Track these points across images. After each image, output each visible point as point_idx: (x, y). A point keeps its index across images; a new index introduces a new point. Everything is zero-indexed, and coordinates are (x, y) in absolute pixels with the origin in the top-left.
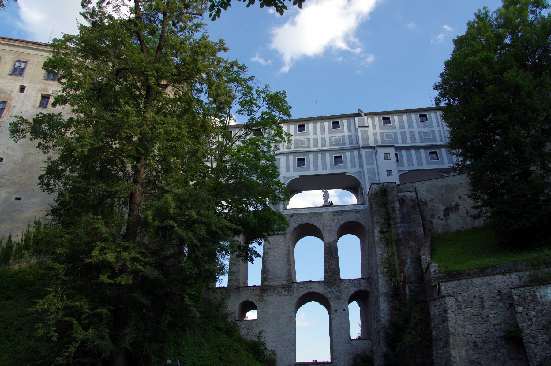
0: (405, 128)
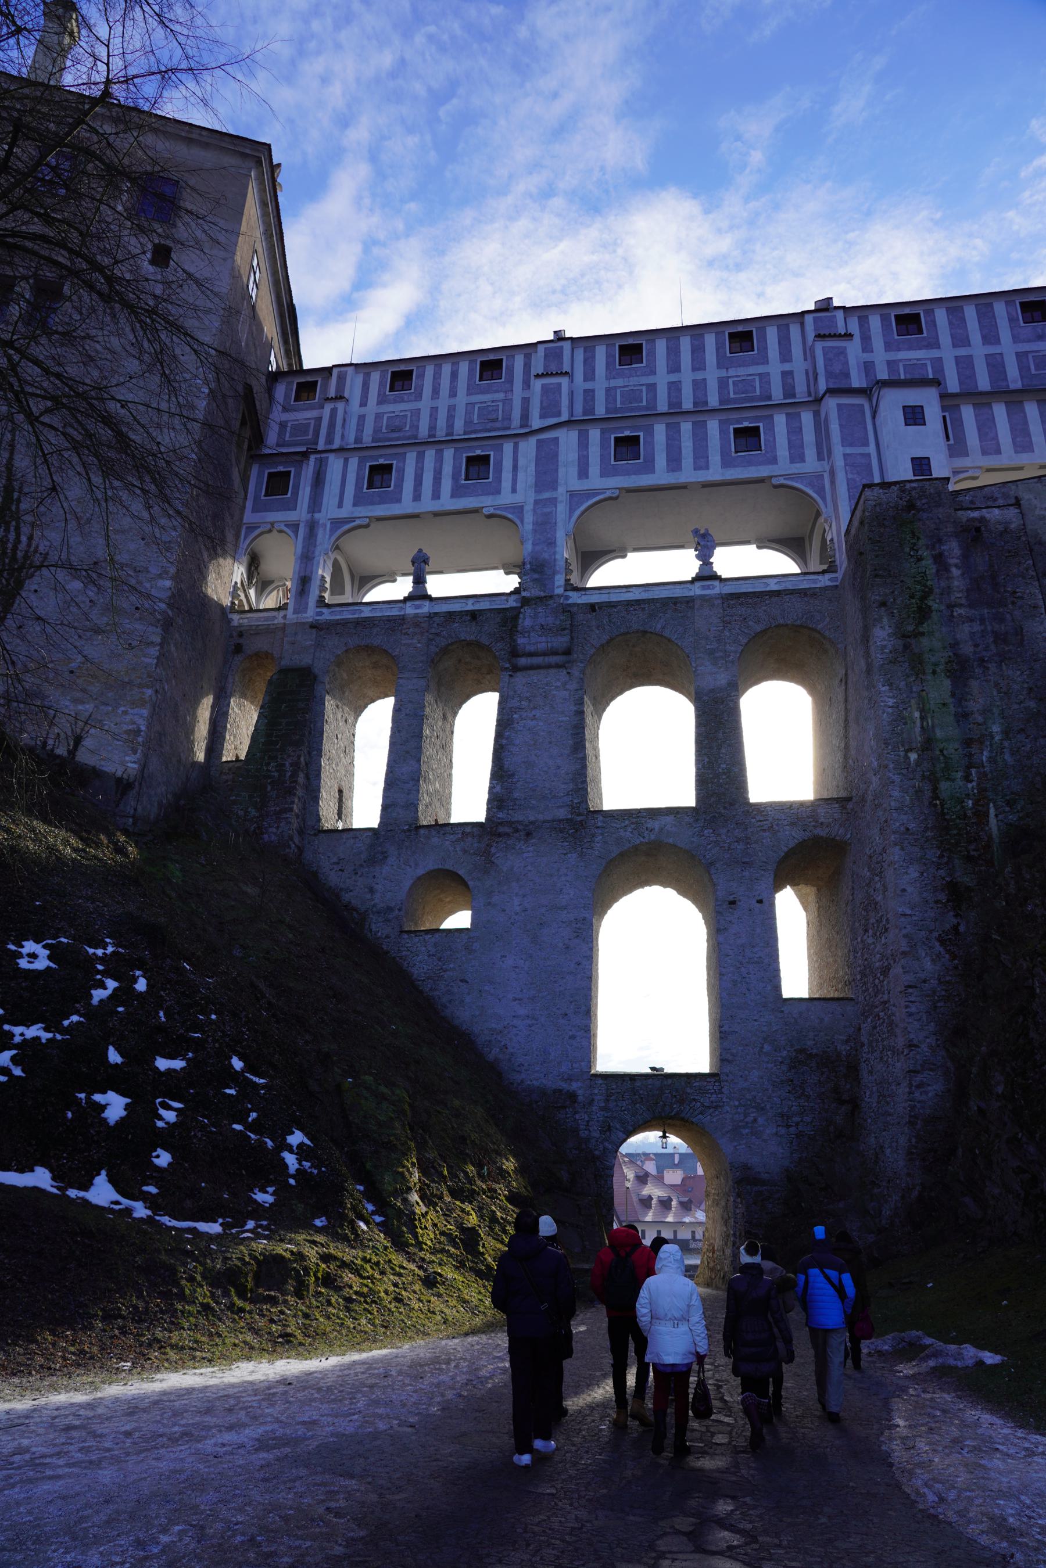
0: (970, 345)
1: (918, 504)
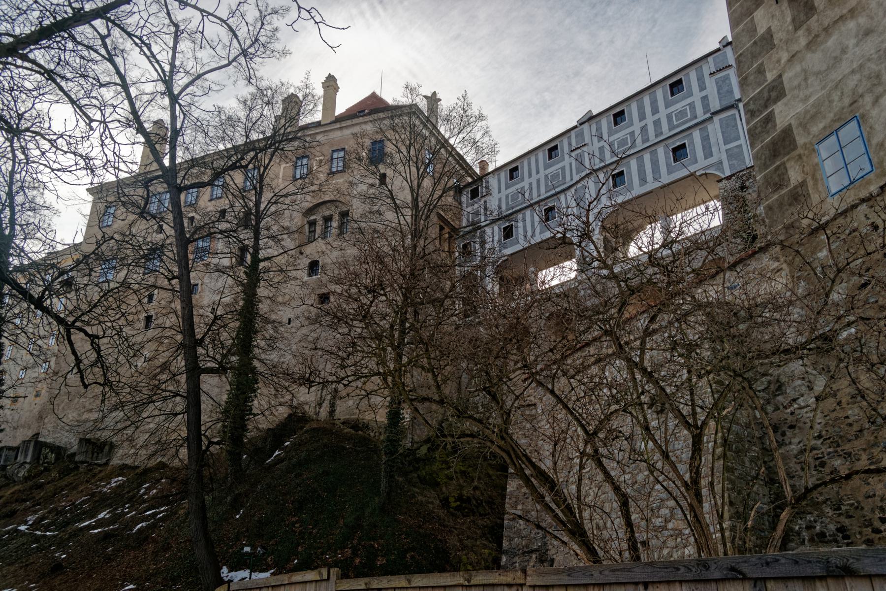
1: (747, 183)
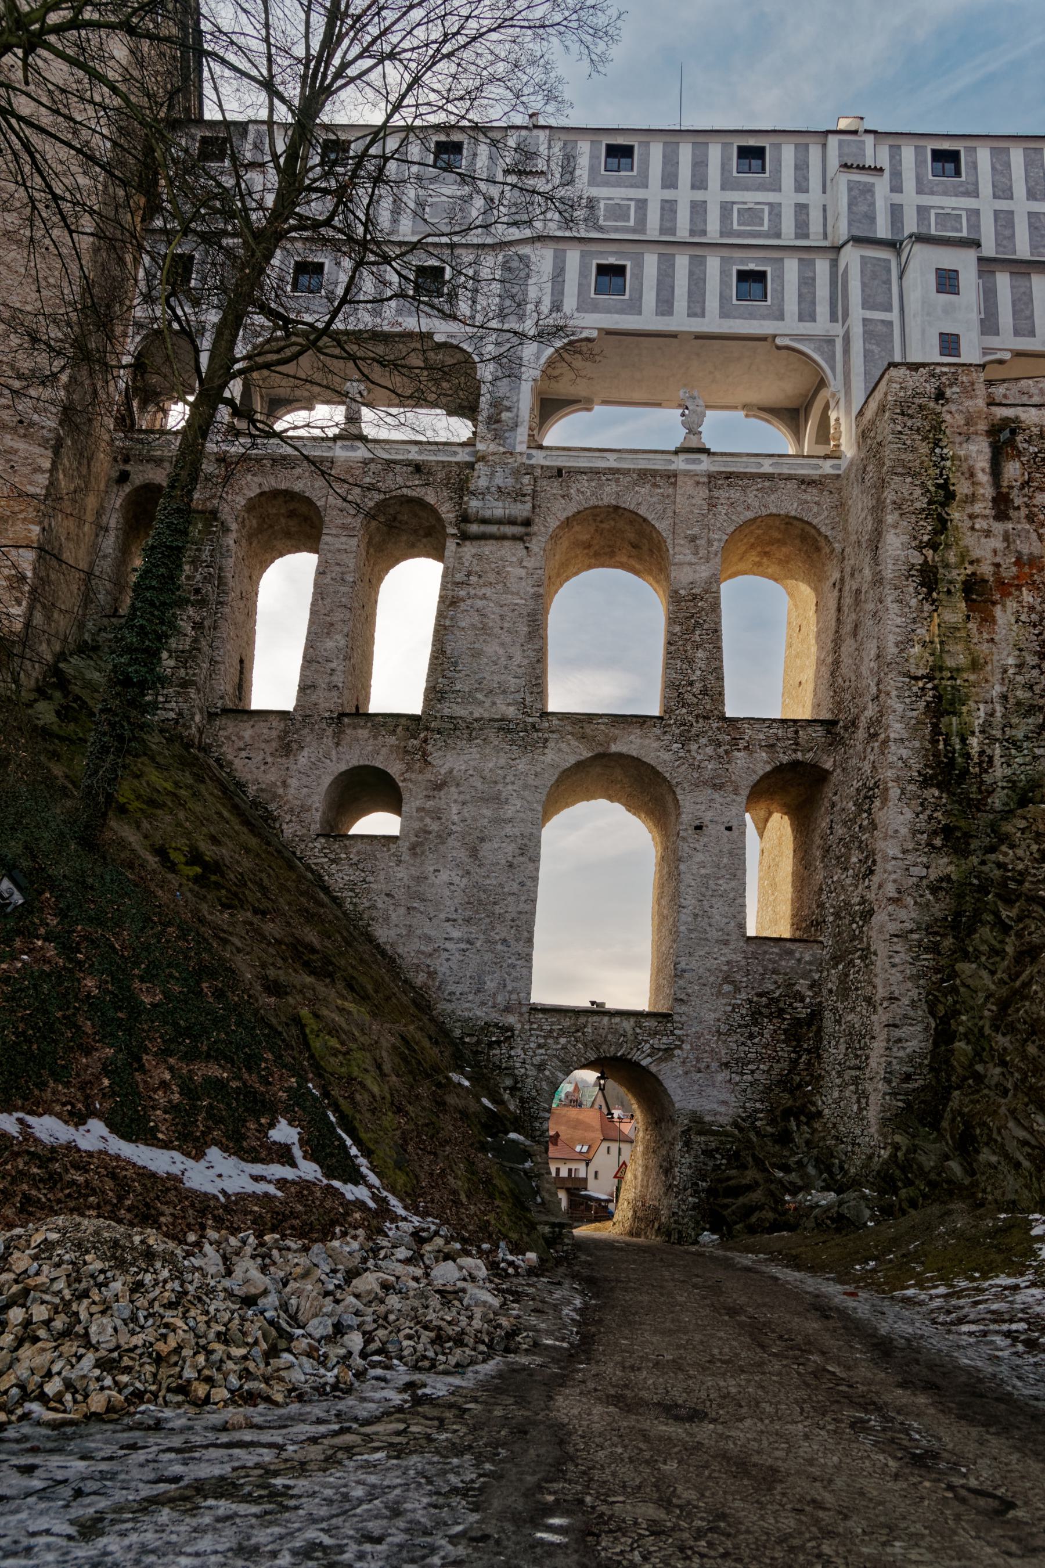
0: (1012, 198)
1: (948, 392)
